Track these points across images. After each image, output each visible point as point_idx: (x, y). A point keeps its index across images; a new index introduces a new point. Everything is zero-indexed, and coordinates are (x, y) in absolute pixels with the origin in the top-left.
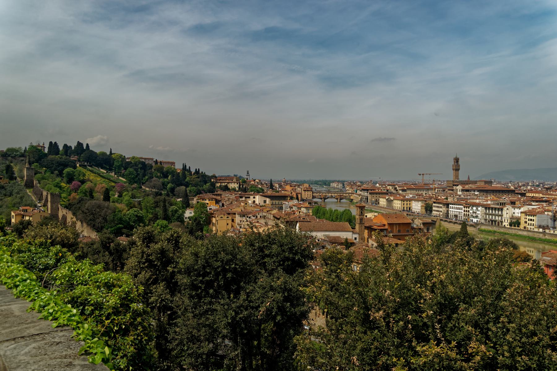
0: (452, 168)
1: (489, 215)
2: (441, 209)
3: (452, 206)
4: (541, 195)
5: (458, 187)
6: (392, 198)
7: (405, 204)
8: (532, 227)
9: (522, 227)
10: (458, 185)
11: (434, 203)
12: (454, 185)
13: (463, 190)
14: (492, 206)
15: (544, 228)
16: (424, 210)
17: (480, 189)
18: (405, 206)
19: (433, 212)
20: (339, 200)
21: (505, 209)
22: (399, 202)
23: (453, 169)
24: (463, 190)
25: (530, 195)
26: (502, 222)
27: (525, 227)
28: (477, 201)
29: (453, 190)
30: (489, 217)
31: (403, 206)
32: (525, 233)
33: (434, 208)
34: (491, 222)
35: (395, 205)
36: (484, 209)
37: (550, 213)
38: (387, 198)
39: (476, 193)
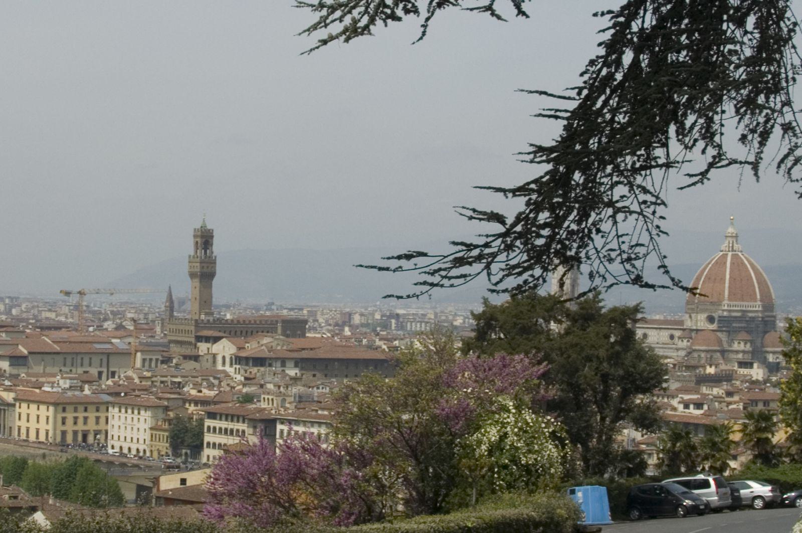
0: (185, 269)
5: (216, 348)
7: (70, 421)
10: (216, 340)
11: (212, 415)
12: (199, 339)
13: (238, 360)
16: (164, 446)
17: (304, 354)
18: (69, 427)
22: (46, 412)
23: (192, 275)
24: (238, 360)
29: (196, 358)
31: (61, 428)
33: (208, 438)
35: (23, 424)
39: (292, 372)
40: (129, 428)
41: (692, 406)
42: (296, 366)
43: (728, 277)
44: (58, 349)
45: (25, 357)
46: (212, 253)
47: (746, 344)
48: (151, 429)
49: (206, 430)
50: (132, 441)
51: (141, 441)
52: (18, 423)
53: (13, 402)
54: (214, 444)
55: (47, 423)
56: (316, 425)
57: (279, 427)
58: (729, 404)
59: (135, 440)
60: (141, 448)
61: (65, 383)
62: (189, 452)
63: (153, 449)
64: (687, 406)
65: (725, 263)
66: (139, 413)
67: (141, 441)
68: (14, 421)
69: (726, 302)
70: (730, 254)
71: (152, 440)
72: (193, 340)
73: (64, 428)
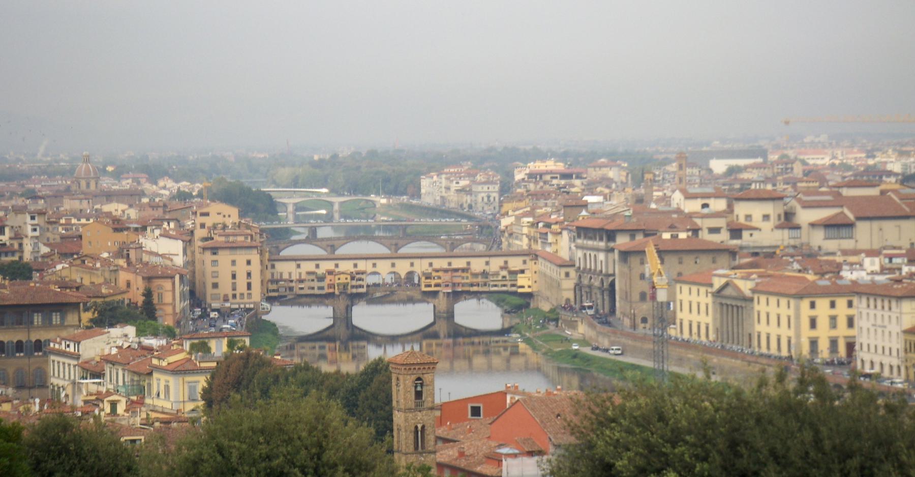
6: (746, 287)
18: (823, 333)
20: (442, 303)
31: (807, 332)
35: (761, 328)
38: (718, 283)
40: (879, 330)
44: (907, 209)
45: (851, 225)
48: (906, 332)
50: (876, 351)
51: (894, 353)
52: (758, 328)
53: (748, 293)
55: (789, 326)
59: (887, 352)
60: (895, 362)
61: (873, 264)
63: (909, 364)
66: (890, 309)
67: (894, 353)
68: (753, 325)
71: (906, 350)
73: (813, 333)
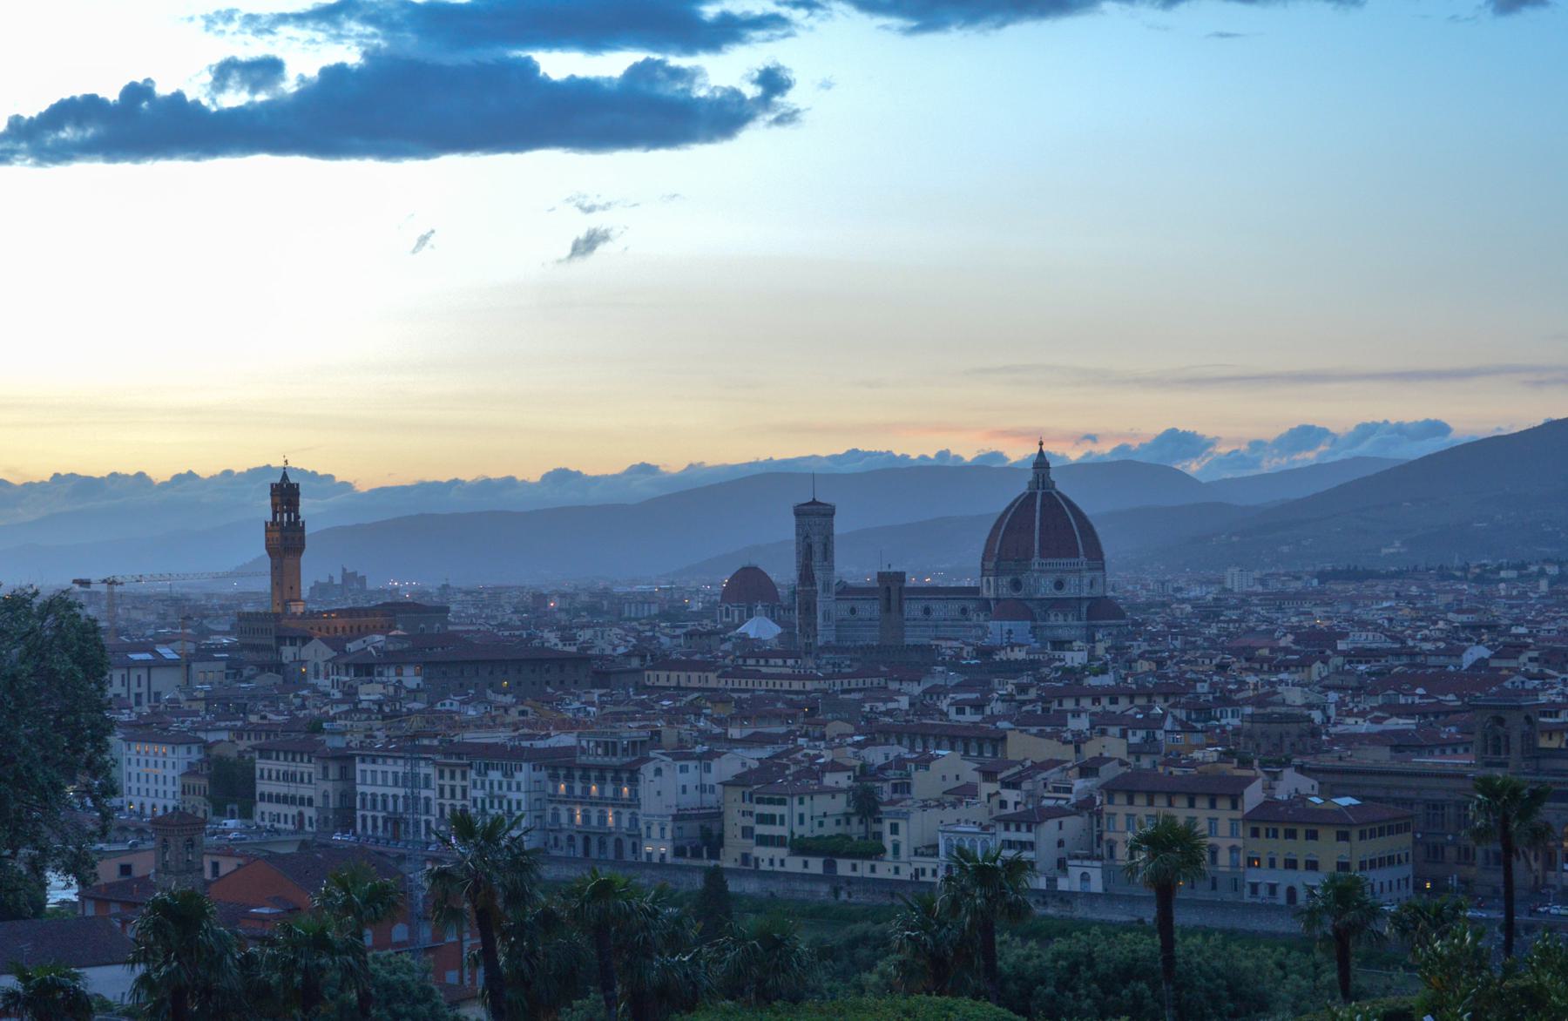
1: (570, 799)
2: (305, 791)
3: (369, 767)
4: (712, 676)
8: (780, 853)
9: (728, 860)
10: (306, 639)
11: (265, 753)
12: (281, 640)
14: (584, 759)
15: (829, 849)
19: (262, 807)
21: (647, 770)
25: (662, 678)
26: (637, 839)
27: (745, 858)
28: (500, 736)
29: (279, 667)
30: (572, 817)
32: (751, 886)
33: (262, 787)
34: (579, 842)
36: (543, 775)
37: (842, 780)
39: (411, 679)
41: (968, 709)
42: (417, 675)
43: (1037, 523)
46: (297, 517)
47: (1066, 615)
49: (258, 773)
51: (170, 795)
54: (270, 795)
56: (390, 761)
57: (359, 766)
58: (1024, 703)
59: (161, 794)
62: (236, 807)
64: (960, 711)
65: (1034, 505)
67: (170, 795)
69: (1036, 559)
70: (1040, 493)
71: (183, 793)
72: (273, 643)
